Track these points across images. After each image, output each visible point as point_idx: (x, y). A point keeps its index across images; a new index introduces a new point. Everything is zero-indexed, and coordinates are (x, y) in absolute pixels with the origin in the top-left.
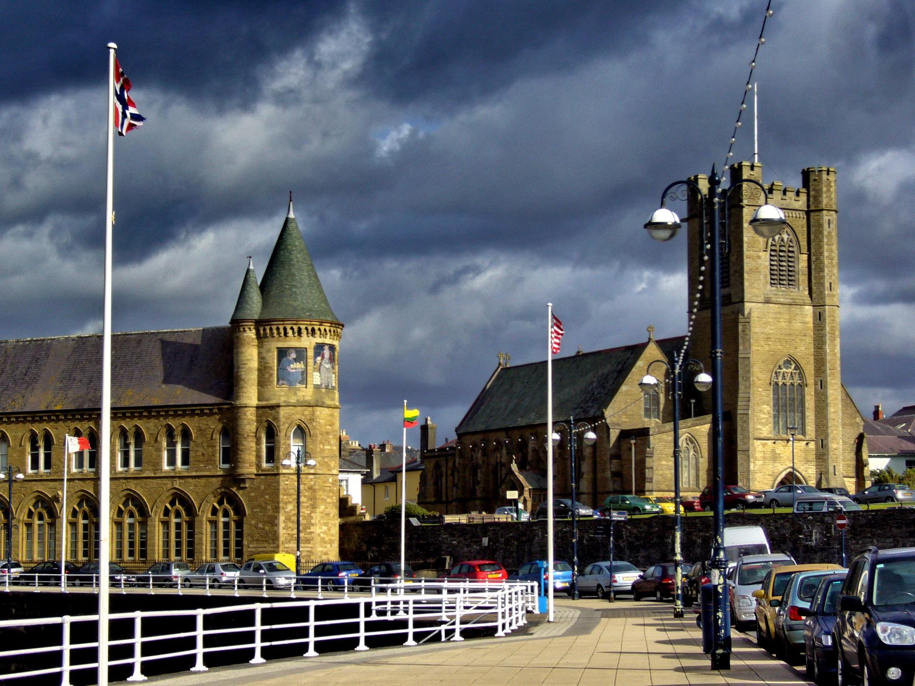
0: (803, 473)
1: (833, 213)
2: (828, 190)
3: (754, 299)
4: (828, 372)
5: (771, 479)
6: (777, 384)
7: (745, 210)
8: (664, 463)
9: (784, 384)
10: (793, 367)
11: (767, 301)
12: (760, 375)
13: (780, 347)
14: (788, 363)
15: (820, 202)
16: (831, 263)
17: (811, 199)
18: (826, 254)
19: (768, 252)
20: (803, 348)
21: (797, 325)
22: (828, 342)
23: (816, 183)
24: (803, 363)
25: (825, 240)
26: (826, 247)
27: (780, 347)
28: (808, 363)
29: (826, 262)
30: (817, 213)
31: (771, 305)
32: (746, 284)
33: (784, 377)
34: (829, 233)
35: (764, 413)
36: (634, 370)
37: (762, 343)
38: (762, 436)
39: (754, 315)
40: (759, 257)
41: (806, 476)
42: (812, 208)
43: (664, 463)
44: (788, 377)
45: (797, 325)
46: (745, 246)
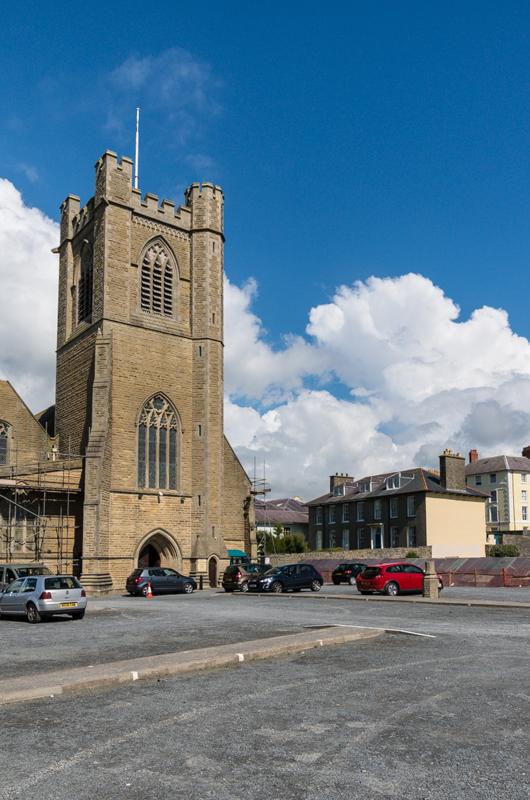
0: (175, 536)
3: (117, 318)
4: (209, 416)
5: (132, 542)
6: (143, 426)
7: (109, 209)
9: (153, 427)
10: (166, 407)
11: (137, 325)
12: (122, 412)
13: (150, 382)
14: (158, 398)
17: (195, 219)
18: (209, 280)
19: (140, 269)
22: (209, 381)
23: (200, 200)
24: (178, 404)
25: (209, 265)
27: (150, 382)
28: (185, 405)
29: (209, 289)
30: (201, 234)
32: (106, 298)
33: (153, 419)
34: (214, 258)
35: (126, 460)
38: (121, 488)
39: (117, 337)
40: (126, 270)
41: (179, 539)
42: (195, 227)
45: (173, 359)
46: (107, 252)
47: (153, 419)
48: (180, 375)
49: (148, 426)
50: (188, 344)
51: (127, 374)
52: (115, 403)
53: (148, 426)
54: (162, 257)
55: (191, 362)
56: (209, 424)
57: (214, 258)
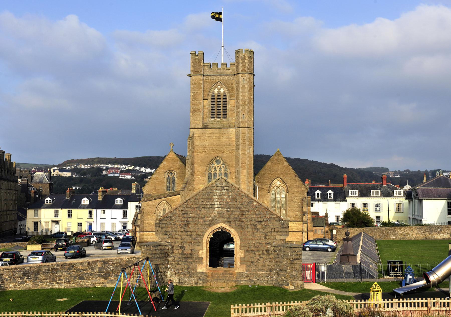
1: (247, 74)
2: (244, 62)
3: (197, 127)
4: (241, 165)
8: (149, 217)
10: (221, 163)
12: (199, 169)
13: (212, 153)
15: (239, 69)
16: (245, 103)
18: (241, 98)
20: (228, 153)
21: (224, 140)
22: (241, 148)
26: (241, 94)
27: (212, 153)
28: (231, 161)
31: (208, 129)
34: (244, 86)
36: (160, 166)
37: (201, 151)
39: (196, 135)
43: (149, 217)
44: (218, 169)
45: (224, 140)
47: (215, 169)
48: (229, 146)
49: (213, 173)
50: (232, 131)
51: (201, 151)
52: (196, 165)
53: (213, 173)
54: (222, 90)
55: (234, 139)
56: (241, 169)
57: (244, 86)
